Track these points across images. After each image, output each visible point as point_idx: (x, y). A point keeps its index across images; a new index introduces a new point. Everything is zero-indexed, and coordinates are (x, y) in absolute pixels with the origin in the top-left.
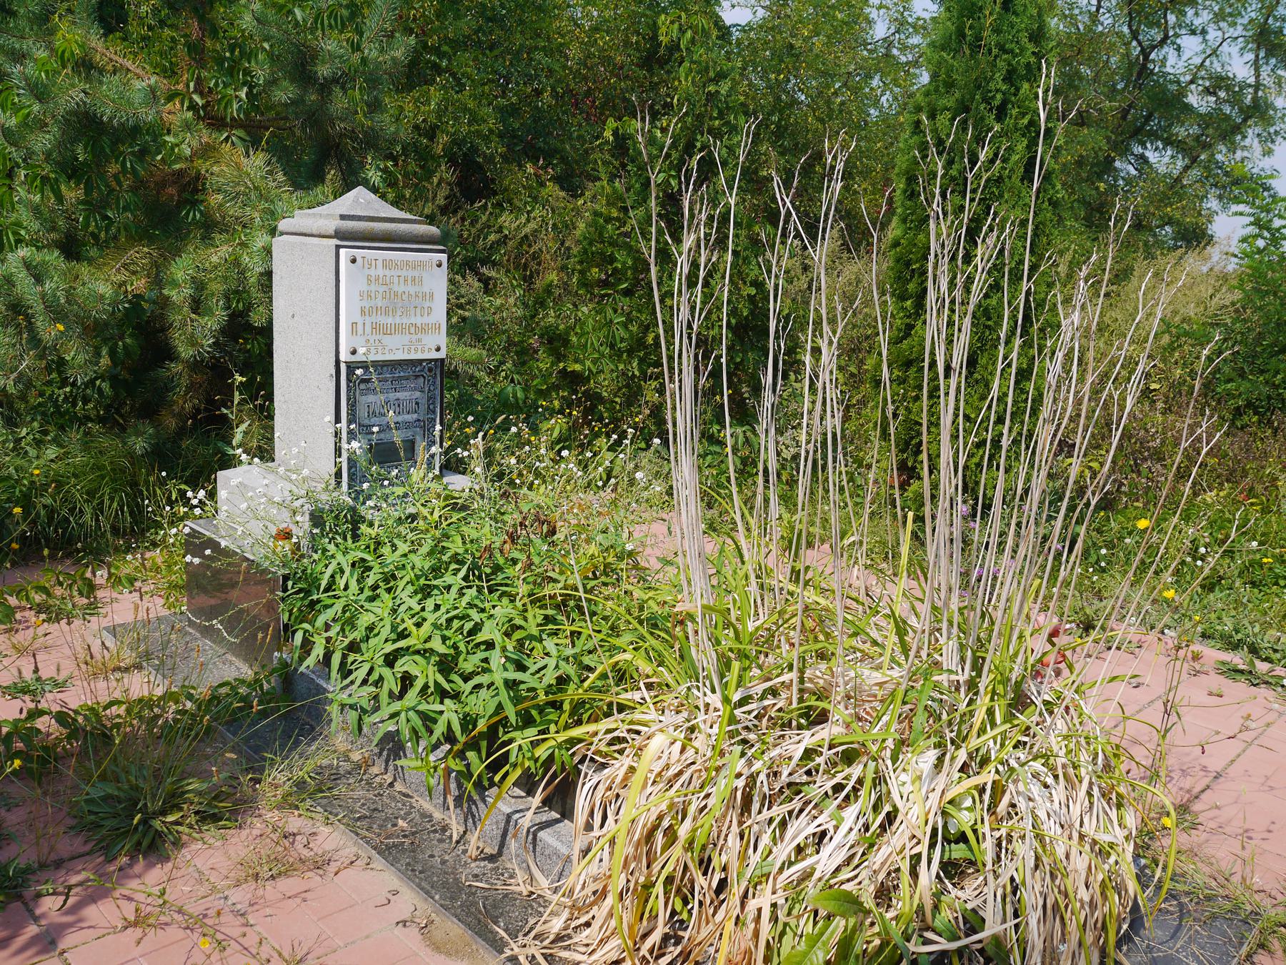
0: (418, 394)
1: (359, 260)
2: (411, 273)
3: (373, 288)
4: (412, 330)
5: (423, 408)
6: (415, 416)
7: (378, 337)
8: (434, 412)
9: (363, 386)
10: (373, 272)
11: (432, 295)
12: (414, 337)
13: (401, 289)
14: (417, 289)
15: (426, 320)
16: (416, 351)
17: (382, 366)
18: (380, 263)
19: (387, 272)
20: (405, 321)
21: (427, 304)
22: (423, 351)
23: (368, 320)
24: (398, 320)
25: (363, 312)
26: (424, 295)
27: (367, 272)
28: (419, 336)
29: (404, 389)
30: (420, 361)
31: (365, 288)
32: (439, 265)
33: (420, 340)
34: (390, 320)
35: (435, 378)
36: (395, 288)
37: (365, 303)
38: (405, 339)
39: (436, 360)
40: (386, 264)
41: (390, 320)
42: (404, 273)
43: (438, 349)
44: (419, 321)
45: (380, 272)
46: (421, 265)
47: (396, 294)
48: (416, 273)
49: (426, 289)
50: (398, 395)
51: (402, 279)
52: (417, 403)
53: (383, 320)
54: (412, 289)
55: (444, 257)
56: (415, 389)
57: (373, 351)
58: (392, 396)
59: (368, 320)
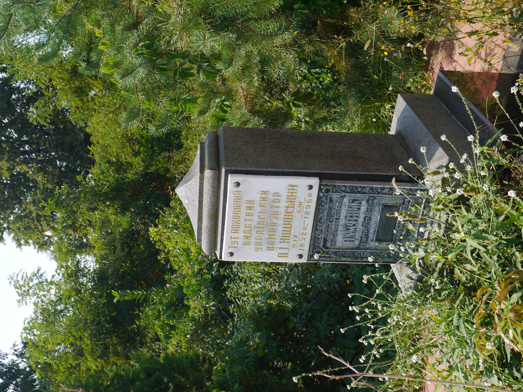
0: (346, 200)
1: (231, 250)
2: (244, 210)
3: (253, 241)
4: (290, 210)
6: (364, 203)
7: (292, 238)
9: (328, 245)
10: (241, 241)
13: (255, 219)
15: (283, 198)
16: (307, 213)
17: (316, 229)
18: (235, 235)
19: (242, 229)
20: (282, 216)
21: (270, 197)
26: (264, 199)
27: (240, 245)
29: (339, 213)
30: (319, 198)
31: (252, 247)
32: (238, 184)
33: (300, 204)
34: (280, 229)
36: (255, 223)
37: (265, 247)
38: (296, 216)
39: (320, 190)
40: (235, 229)
42: (243, 216)
44: (283, 204)
45: (241, 235)
46: (237, 200)
48: (244, 206)
49: (257, 197)
51: (248, 218)
53: (279, 234)
54: (257, 209)
55: (232, 179)
57: (303, 242)
58: (342, 221)
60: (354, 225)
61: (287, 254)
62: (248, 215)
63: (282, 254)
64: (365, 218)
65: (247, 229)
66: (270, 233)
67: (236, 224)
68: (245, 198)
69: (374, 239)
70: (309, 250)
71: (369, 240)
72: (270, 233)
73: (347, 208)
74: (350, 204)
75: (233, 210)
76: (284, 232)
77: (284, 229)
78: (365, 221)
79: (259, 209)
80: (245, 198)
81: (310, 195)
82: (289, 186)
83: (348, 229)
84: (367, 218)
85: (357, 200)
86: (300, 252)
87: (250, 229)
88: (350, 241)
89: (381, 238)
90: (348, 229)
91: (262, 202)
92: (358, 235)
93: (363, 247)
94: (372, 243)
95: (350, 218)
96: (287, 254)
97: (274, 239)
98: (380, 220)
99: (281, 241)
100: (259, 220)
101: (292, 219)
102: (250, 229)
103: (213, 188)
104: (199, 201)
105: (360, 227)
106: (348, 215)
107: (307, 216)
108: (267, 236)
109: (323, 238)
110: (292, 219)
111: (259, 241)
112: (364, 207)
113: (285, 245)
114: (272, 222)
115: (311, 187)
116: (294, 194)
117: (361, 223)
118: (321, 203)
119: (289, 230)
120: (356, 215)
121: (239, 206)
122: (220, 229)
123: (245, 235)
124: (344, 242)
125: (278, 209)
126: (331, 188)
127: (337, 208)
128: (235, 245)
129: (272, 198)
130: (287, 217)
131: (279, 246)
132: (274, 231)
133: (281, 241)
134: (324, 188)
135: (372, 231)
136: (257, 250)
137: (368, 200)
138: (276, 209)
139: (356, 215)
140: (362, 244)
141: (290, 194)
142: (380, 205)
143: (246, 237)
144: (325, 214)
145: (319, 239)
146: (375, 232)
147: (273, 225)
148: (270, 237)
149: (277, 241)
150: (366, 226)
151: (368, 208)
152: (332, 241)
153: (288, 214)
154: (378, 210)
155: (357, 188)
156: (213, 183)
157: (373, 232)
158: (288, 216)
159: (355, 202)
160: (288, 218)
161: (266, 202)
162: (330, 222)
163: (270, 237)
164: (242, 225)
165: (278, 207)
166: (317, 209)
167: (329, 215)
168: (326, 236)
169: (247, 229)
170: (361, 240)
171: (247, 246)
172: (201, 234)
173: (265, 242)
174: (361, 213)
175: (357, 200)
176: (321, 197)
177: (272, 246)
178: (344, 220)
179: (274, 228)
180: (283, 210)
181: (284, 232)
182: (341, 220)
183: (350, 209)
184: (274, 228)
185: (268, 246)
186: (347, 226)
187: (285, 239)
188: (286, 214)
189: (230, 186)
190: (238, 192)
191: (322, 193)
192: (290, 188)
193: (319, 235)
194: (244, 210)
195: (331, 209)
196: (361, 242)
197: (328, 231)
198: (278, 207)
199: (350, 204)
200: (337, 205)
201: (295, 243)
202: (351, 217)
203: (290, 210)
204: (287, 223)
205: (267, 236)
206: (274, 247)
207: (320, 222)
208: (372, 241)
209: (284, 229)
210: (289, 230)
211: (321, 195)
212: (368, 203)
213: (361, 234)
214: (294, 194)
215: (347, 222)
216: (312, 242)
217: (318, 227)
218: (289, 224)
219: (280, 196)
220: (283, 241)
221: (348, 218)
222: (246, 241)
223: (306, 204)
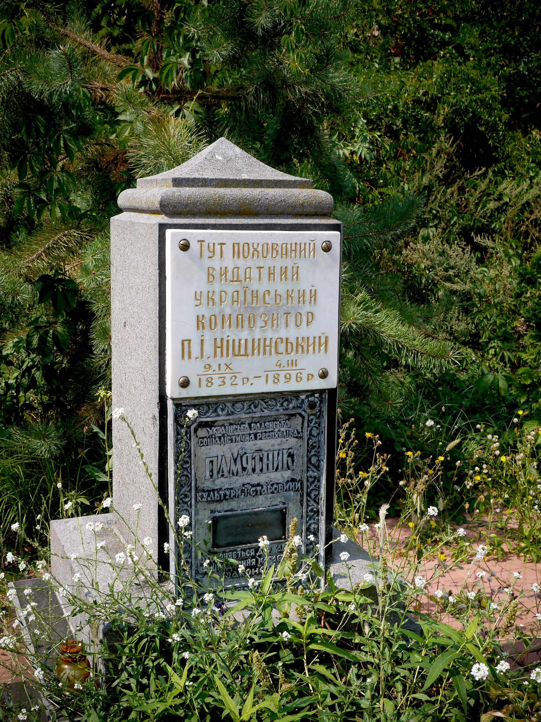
0: (292, 441)
1: (194, 246)
2: (279, 263)
3: (217, 287)
4: (282, 348)
5: (301, 461)
6: (288, 474)
7: (225, 360)
8: (318, 467)
9: (202, 432)
10: (216, 263)
11: (314, 295)
12: (284, 359)
13: (264, 286)
14: (290, 286)
15: (304, 331)
16: (288, 379)
17: (234, 403)
18: (228, 250)
19: (241, 263)
20: (269, 334)
21: (307, 308)
22: (299, 379)
23: (209, 336)
24: (257, 334)
25: (200, 323)
26: (302, 295)
27: (207, 263)
28: (293, 356)
29: (269, 434)
30: (296, 394)
31: (203, 286)
32: (327, 249)
33: (294, 363)
34: (244, 335)
35: (320, 417)
36: (254, 286)
37: (204, 311)
38: (271, 361)
39: (322, 392)
41: (244, 335)
42: (268, 262)
43: (324, 375)
44: (292, 333)
45: (229, 262)
47: (255, 294)
48: (288, 263)
49: (305, 285)
50: (259, 443)
51: (265, 272)
52: (291, 456)
54: (281, 287)
55: (335, 237)
56: (288, 434)
57: (217, 381)
58: (250, 445)
59: (209, 336)
60: (244, 469)
61: (190, 357)
62: (271, 273)
63: (189, 347)
64: (258, 485)
65: (242, 272)
66: (234, 318)
67: (251, 250)
68: (302, 264)
69: (217, 514)
70: (196, 398)
71: (213, 506)
72: (234, 318)
73: (276, 447)
74: (285, 451)
75: (280, 243)
76: (237, 344)
77: (243, 342)
78: (253, 486)
79: (282, 291)
80: (302, 264)
81: (310, 376)
82: (326, 338)
83: (235, 460)
84: (259, 488)
85: (293, 461)
86: (194, 381)
87: (242, 277)
88: (212, 471)
89: (220, 527)
90: (235, 460)
91: (295, 295)
92: (220, 483)
93: (199, 498)
94: (208, 513)
95: (257, 458)
96: (190, 357)
97: (223, 327)
98: (256, 514)
99: (219, 341)
100: (261, 294)
101: (264, 353)
102: (242, 277)
103: (302, 205)
104: (261, 181)
105: (237, 482)
106: (265, 454)
107: (271, 379)
108: (228, 311)
109: (217, 418)
110: (264, 353)
111: (217, 298)
112: (278, 477)
113: (208, 348)
114: (258, 318)
115: (324, 375)
116: (311, 348)
117: (247, 481)
118: (286, 400)
119: (242, 352)
120: (265, 467)
121: (286, 254)
122: (212, 221)
123: (230, 269)
124: (208, 460)
125: (284, 325)
126: (317, 409)
127: (276, 430)
128: (206, 253)
129: (304, 312)
130: (268, 343)
131: (206, 338)
132: (239, 324)
133: (219, 341)
134: (316, 398)
135: (233, 504)
136: (197, 297)
137: (293, 480)
138: (283, 321)
139: (265, 467)
140: (205, 495)
141: (311, 341)
142: (284, 503)
143: (226, 273)
144: (266, 411)
145: (215, 411)
146: (231, 510)
147: (252, 321)
148: (227, 317)
149: (218, 333)
150: (243, 491)
151: (277, 484)
152: (211, 437)
153: (273, 344)
154: (274, 503)
155: (317, 455)
156: (310, 205)
157: (230, 508)
158: (270, 346)
159: (290, 459)
160: (265, 346)
161: (295, 302)
162: (250, 425)
163: (227, 317)
164: (250, 262)
165: (287, 326)
166: (282, 395)
167: (263, 420)
168: (220, 423)
169: (242, 272)
170: (213, 490)
171: (205, 276)
172: (193, 186)
173: (216, 310)
174: (268, 474)
175: (293, 461)
176: (297, 398)
177: (207, 325)
178: (255, 448)
179: (246, 323)
180: (283, 333)
181: (237, 344)
182: (252, 443)
183: (276, 453)
184: (246, 323)
185: (207, 317)
186: (241, 457)
187: (221, 347)
188: (274, 340)
189: (324, 235)
190: (314, 250)
191: (307, 397)
192: (323, 340)
193: (222, 410)
194: (279, 263)
195: (275, 420)
196: (209, 491)
197: (231, 424)
198: (287, 326)
199: (285, 451)
200: (283, 429)
201: (215, 367)
202: (261, 459)
203: (282, 348)
204: (256, 345)
205: (228, 311)
206: (203, 328)
207: (250, 406)
208: (212, 512)
209: (243, 342)
210: (242, 352)
211: (303, 397)
212: (288, 482)
213: (227, 486)
214: (311, 348)
215: (250, 456)
216: (214, 400)
217: (239, 405)
218: (253, 350)
219: (308, 325)
220: (219, 344)
221: (257, 456)
222: (217, 274)
223: (293, 374)
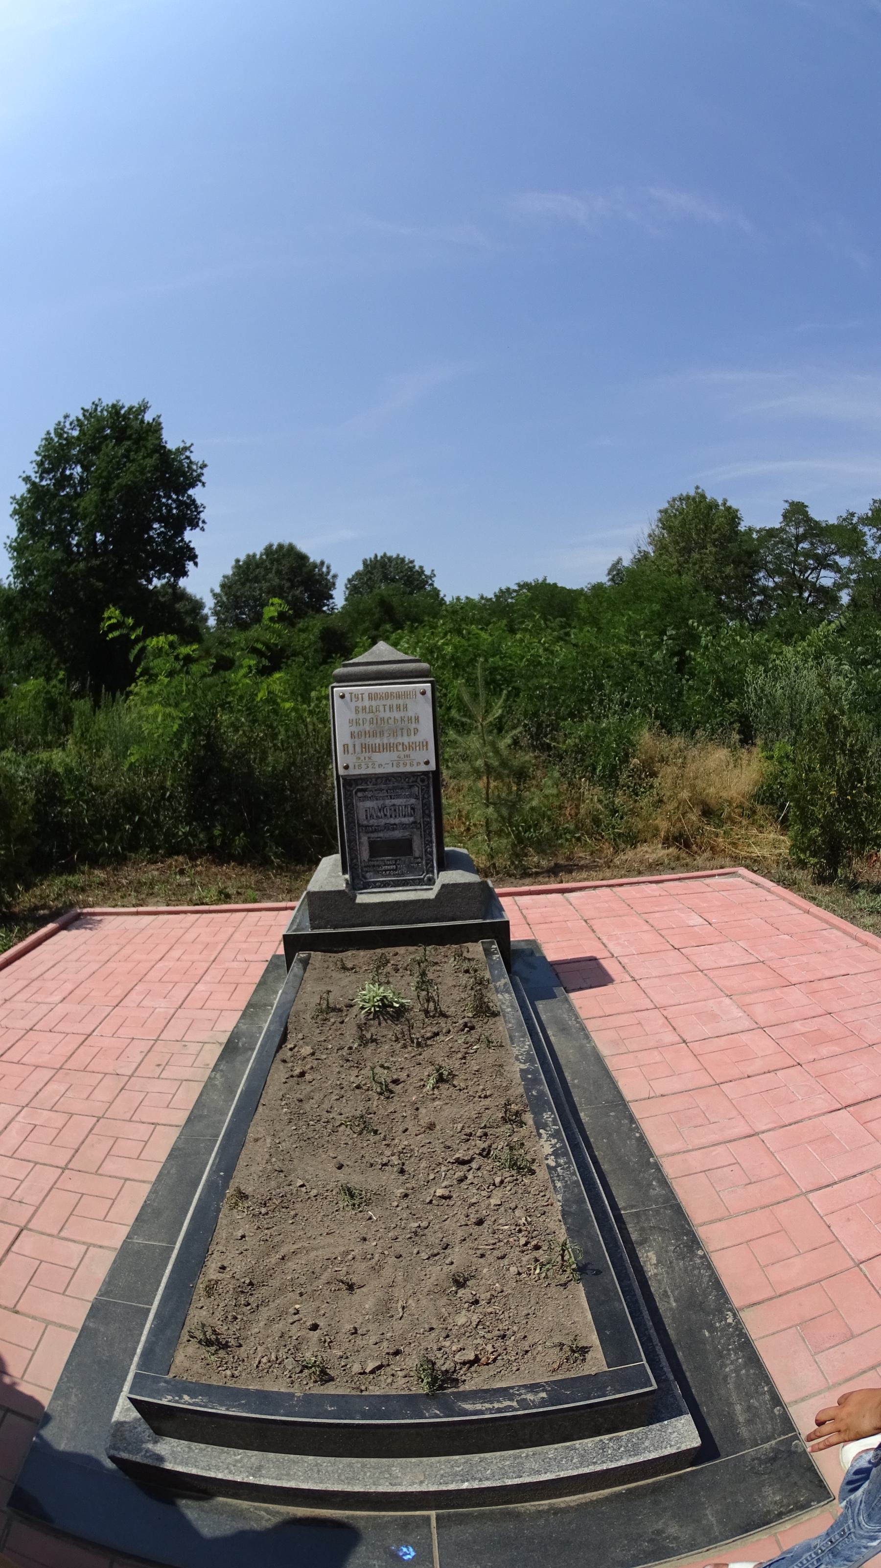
0: (413, 801)
1: (347, 696)
2: (395, 702)
3: (361, 716)
4: (400, 748)
5: (419, 812)
6: (412, 819)
7: (367, 755)
8: (430, 816)
9: (360, 794)
10: (360, 704)
11: (417, 719)
12: (402, 754)
13: (387, 715)
14: (402, 714)
15: (413, 739)
18: (366, 697)
19: (374, 703)
20: (392, 741)
21: (414, 726)
22: (412, 765)
23: (358, 742)
24: (385, 741)
25: (352, 735)
26: (410, 719)
28: (407, 752)
31: (353, 716)
34: (378, 741)
35: (428, 786)
36: (382, 714)
37: (356, 729)
38: (394, 755)
40: (371, 697)
41: (378, 741)
42: (389, 702)
43: (427, 763)
44: (406, 740)
45: (367, 703)
46: (406, 695)
47: (382, 719)
48: (400, 702)
49: (411, 713)
50: (395, 801)
52: (413, 809)
53: (370, 741)
54: (397, 715)
56: (410, 796)
58: (388, 802)
59: (358, 742)
60: (385, 815)
62: (391, 708)
71: (369, 835)
80: (408, 701)
86: (351, 766)
91: (406, 719)
92: (373, 822)
105: (383, 822)
111: (361, 722)
112: (406, 820)
113: (358, 749)
126: (426, 783)
128: (354, 699)
132: (374, 735)
135: (381, 835)
149: (362, 740)
155: (429, 809)
161: (406, 723)
164: (378, 702)
180: (400, 740)
194: (395, 702)
201: (362, 758)
203: (400, 748)
222: (360, 709)
